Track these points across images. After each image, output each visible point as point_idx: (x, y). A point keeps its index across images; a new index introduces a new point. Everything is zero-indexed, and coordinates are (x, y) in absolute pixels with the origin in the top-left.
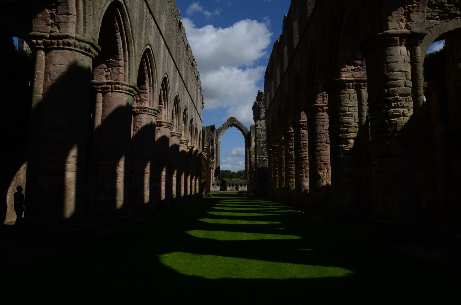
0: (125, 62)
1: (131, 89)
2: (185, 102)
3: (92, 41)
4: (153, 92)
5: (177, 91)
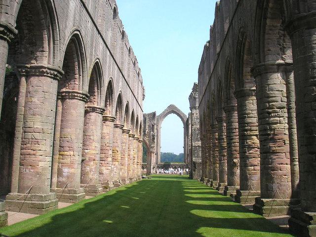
0: (80, 75)
1: (84, 96)
2: (127, 98)
3: (59, 69)
4: (101, 94)
5: (120, 90)
